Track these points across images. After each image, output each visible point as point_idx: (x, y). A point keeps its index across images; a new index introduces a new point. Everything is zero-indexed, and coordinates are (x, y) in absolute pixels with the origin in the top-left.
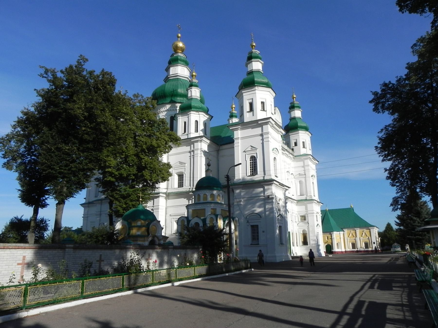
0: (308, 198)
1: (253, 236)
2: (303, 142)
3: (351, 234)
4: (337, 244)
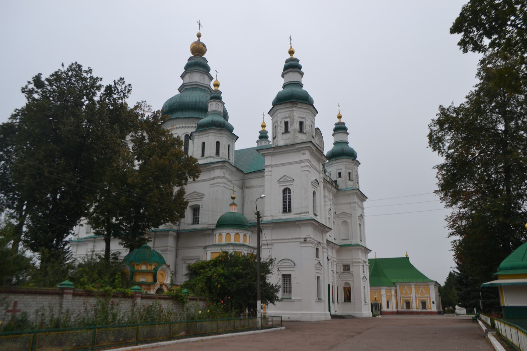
1: (285, 287)
2: (349, 173)
4: (388, 302)
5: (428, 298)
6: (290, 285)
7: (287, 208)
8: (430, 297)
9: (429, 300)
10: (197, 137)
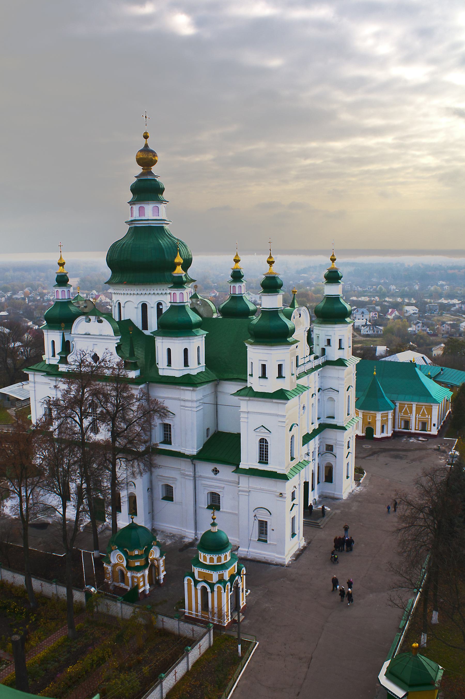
2: (340, 340)
3: (405, 408)
4: (383, 427)
5: (429, 420)
6: (266, 528)
8: (431, 419)
9: (429, 421)
10: (161, 341)
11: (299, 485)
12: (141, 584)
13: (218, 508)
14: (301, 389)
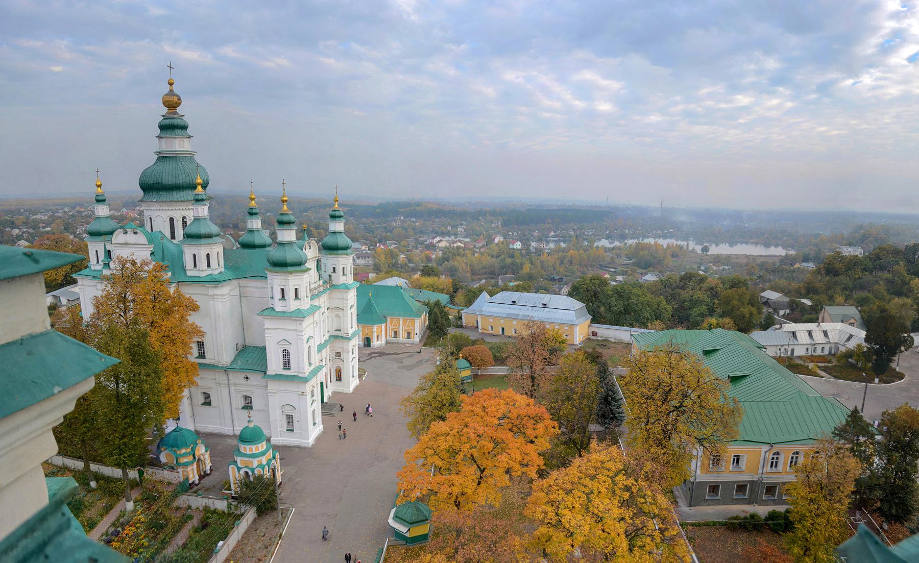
0: (344, 335)
2: (343, 268)
4: (378, 336)
7: (287, 365)
11: (317, 384)
12: (191, 476)
13: (251, 408)
14: (314, 309)
